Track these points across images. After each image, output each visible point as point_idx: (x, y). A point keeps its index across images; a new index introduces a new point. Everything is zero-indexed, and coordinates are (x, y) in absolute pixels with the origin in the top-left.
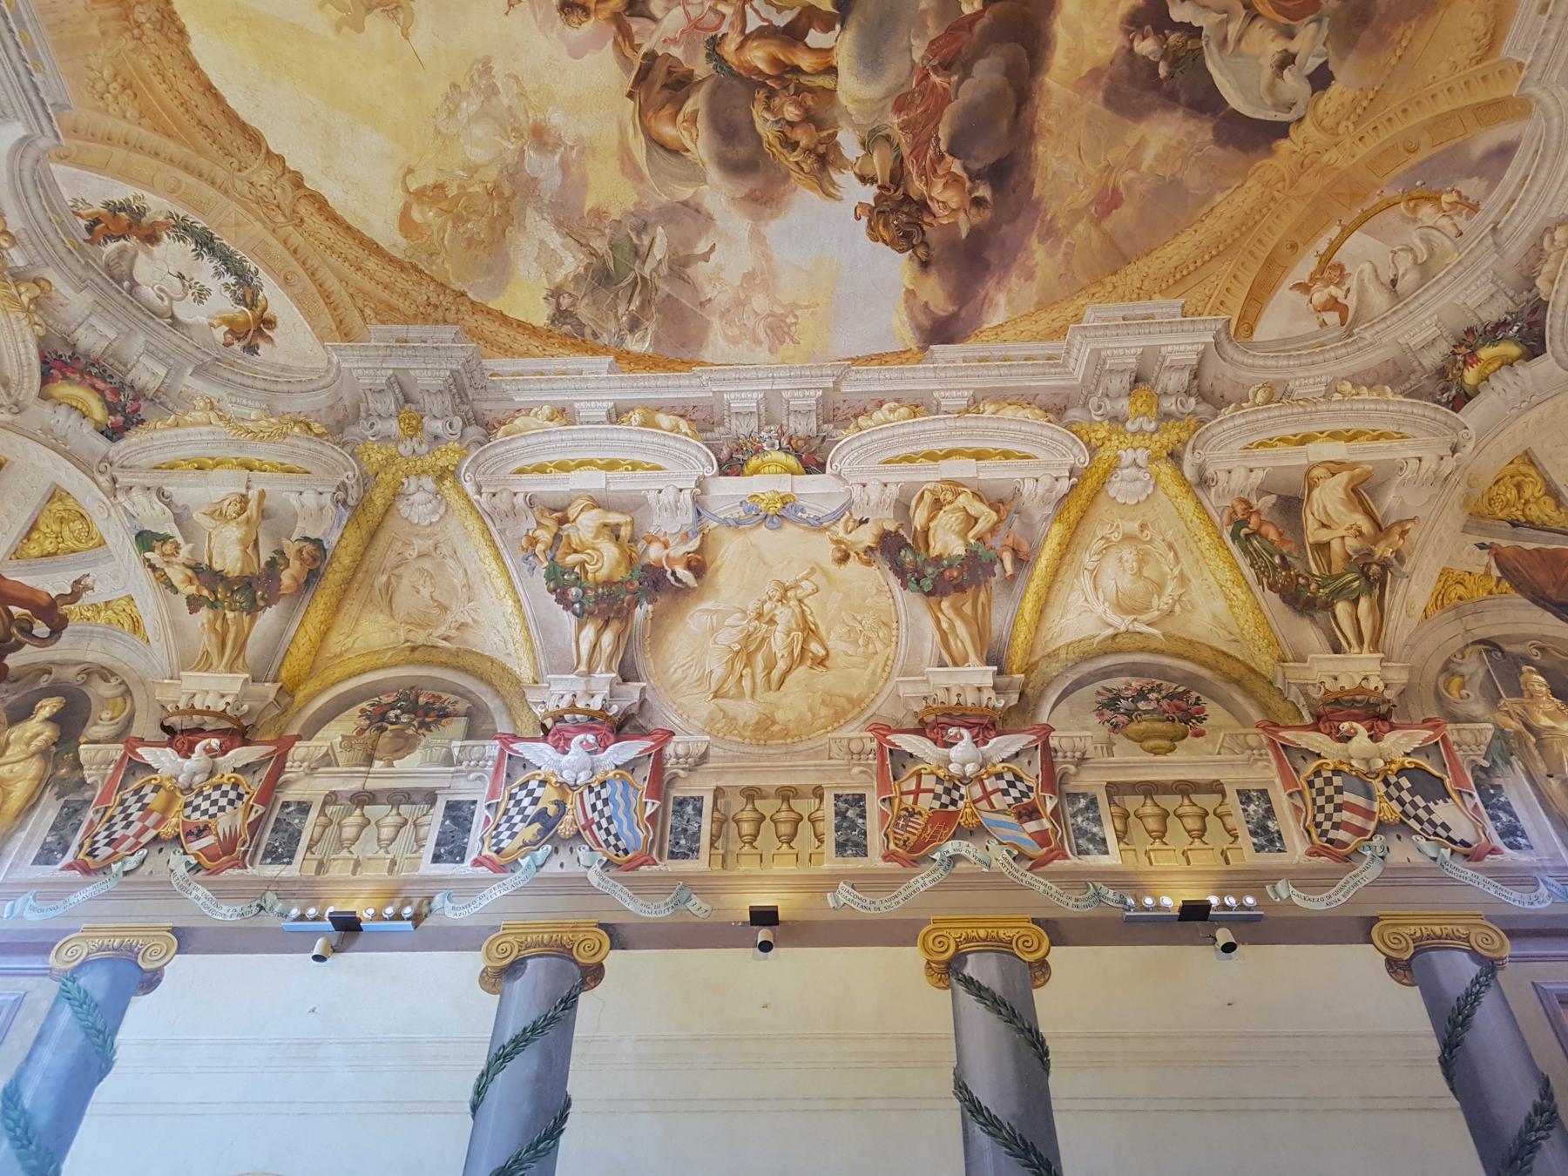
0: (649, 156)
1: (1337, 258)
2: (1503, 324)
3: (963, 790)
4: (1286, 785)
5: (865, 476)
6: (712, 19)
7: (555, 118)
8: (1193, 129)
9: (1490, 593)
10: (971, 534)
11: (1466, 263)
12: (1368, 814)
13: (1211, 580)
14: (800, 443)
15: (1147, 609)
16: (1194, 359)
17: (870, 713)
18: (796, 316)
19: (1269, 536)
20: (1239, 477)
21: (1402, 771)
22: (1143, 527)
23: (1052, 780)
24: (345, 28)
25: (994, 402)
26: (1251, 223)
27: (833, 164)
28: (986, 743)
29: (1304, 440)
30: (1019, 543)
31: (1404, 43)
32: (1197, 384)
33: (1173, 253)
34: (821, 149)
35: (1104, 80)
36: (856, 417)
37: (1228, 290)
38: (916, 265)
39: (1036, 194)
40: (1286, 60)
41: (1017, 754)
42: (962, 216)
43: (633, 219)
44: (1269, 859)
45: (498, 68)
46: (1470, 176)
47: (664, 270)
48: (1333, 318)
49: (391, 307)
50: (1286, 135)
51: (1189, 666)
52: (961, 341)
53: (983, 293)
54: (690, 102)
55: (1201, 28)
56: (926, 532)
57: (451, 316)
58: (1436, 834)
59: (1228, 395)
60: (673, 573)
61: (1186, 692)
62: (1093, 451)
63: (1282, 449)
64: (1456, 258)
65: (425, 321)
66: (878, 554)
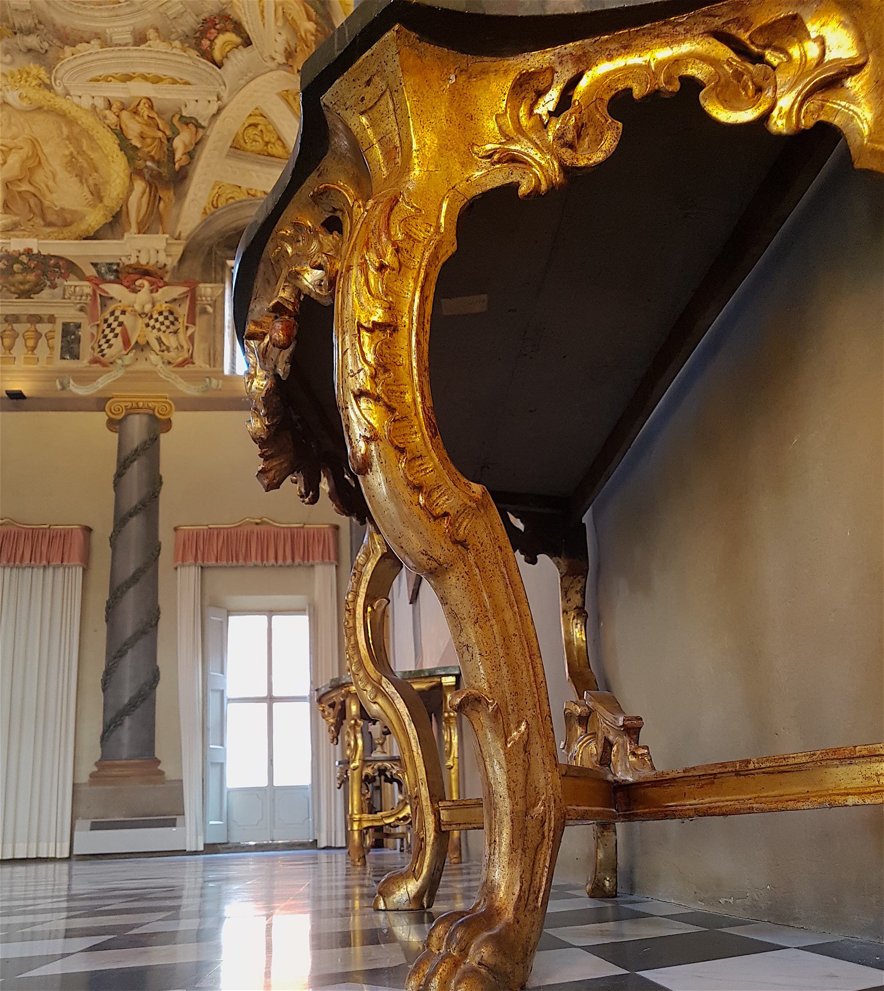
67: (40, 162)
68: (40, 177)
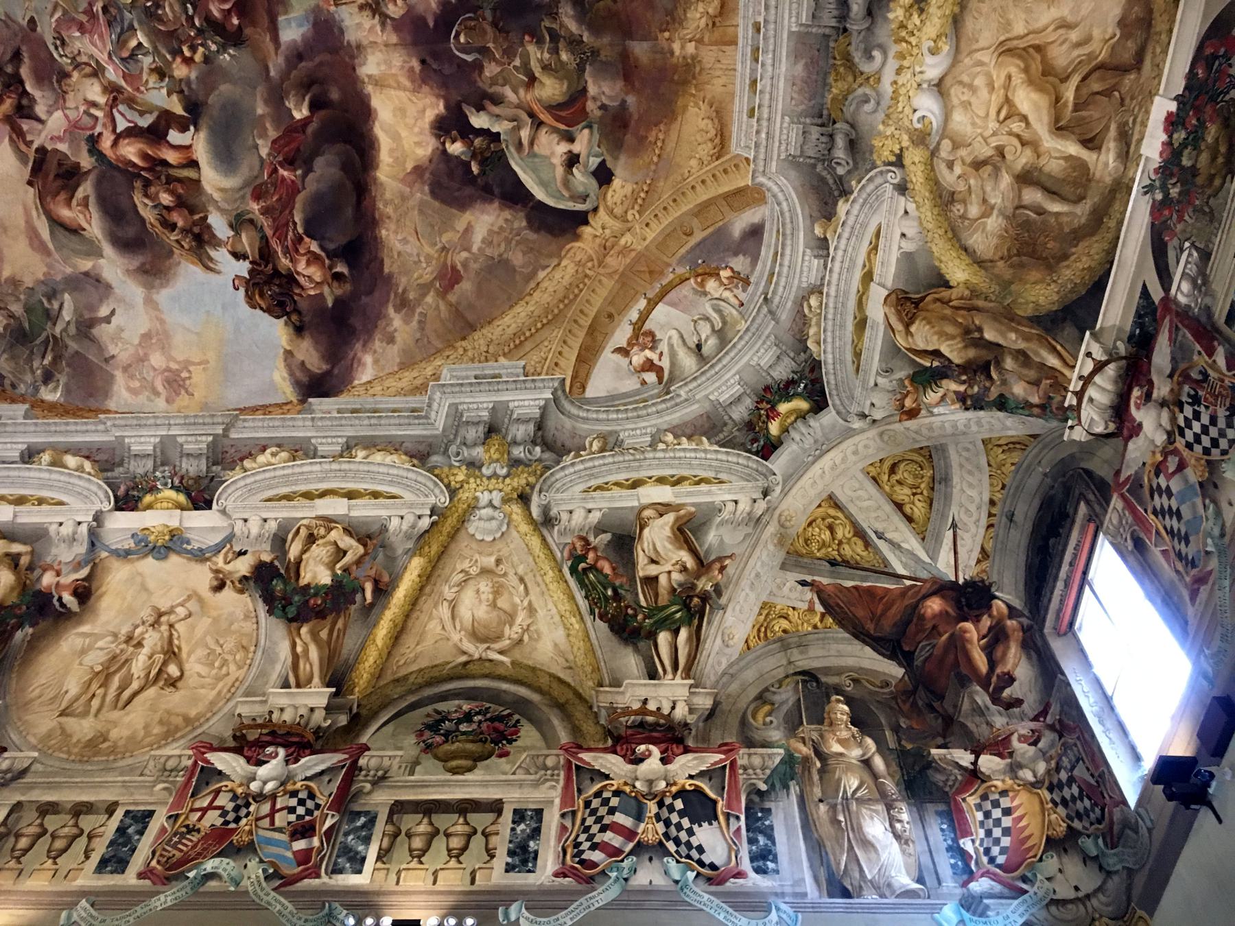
0: (52, 233)
1: (647, 326)
2: (791, 383)
3: (252, 809)
4: (564, 803)
5: (247, 512)
6: (87, 121)
8: (509, 217)
9: (815, 627)
10: (338, 566)
11: (753, 330)
12: (629, 834)
13: (554, 611)
14: (191, 482)
15: (499, 637)
16: (536, 412)
17: (199, 731)
19: (605, 574)
20: (578, 518)
21: (681, 793)
22: (498, 562)
23: (344, 801)
25: (365, 448)
26: (571, 297)
28: (297, 761)
29: (636, 484)
30: (380, 575)
31: (659, 144)
32: (542, 435)
33: (512, 321)
34: (196, 230)
35: (427, 175)
36: (242, 460)
38: (291, 330)
39: (386, 270)
40: (572, 160)
41: (322, 773)
42: (326, 290)
43: (43, 288)
44: (519, 880)
46: (736, 254)
47: (72, 330)
48: (651, 377)
50: (586, 223)
51: (523, 691)
53: (352, 354)
54: (81, 189)
55: (498, 134)
56: (298, 563)
58: (689, 857)
59: (568, 444)
60: (60, 599)
61: (510, 715)
62: (453, 493)
63: (617, 491)
64: (743, 326)
66: (252, 583)
67: (1038, 48)
68: (1061, 56)
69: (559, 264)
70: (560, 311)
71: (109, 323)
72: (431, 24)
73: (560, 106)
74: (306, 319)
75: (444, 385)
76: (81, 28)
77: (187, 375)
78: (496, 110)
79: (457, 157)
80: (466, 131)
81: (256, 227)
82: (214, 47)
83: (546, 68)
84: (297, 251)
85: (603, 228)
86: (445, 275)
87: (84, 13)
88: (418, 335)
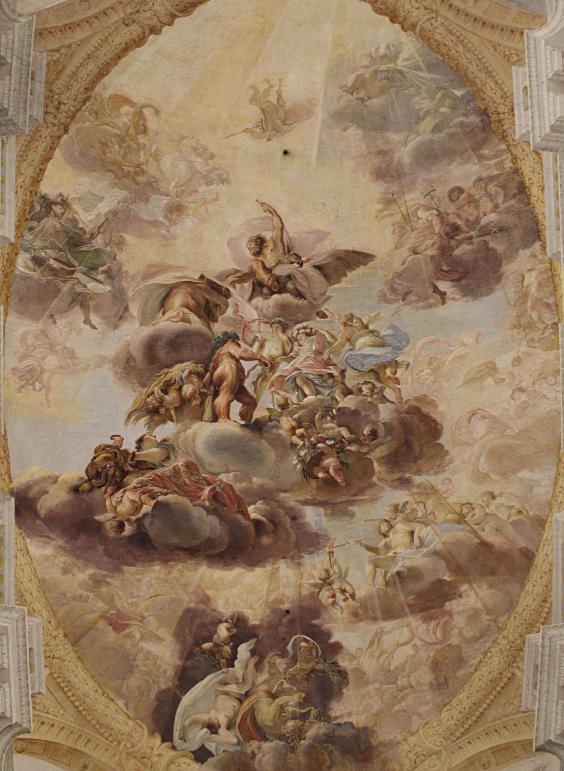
7: (188, 222)
8: (168, 674)
18: (40, 390)
24: (252, 92)
26: (102, 731)
27: (152, 419)
34: (162, 410)
35: (202, 607)
37: (53, 725)
38: (76, 483)
39: (126, 568)
40: (213, 728)
42: (110, 515)
43: (116, 269)
45: (223, 188)
47: (79, 289)
49: (59, 73)
50: (163, 741)
52: (16, 521)
53: (53, 536)
55: (233, 666)
57: (50, 118)
65: (47, 98)
69: (129, 718)
70: (89, 721)
71: (85, 322)
72: (315, 622)
73: (254, 719)
74: (85, 496)
75: (24, 620)
76: (319, 353)
77: (37, 388)
78: (251, 666)
79: (216, 631)
80: (236, 640)
81: (163, 461)
82: (302, 453)
83: (282, 708)
84: (143, 493)
85: (159, 755)
86: (121, 619)
87: (329, 358)
88: (69, 595)
